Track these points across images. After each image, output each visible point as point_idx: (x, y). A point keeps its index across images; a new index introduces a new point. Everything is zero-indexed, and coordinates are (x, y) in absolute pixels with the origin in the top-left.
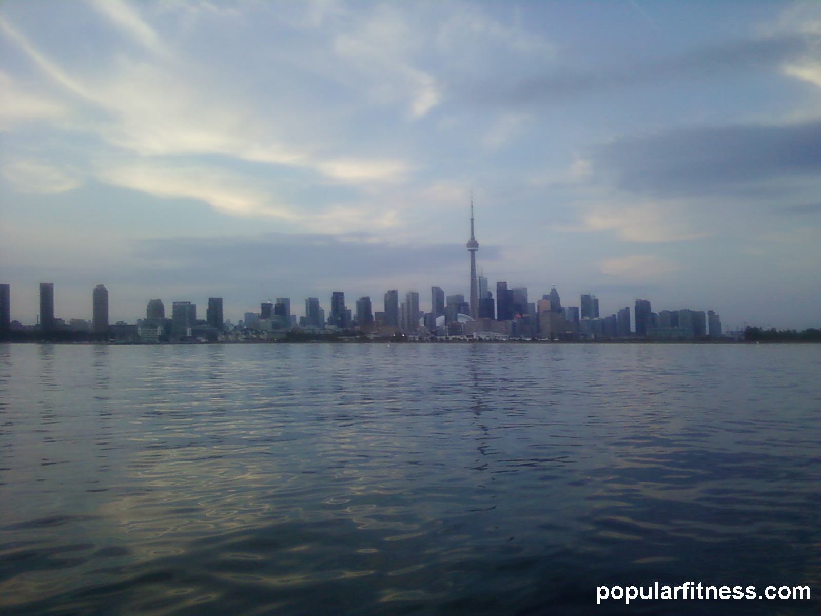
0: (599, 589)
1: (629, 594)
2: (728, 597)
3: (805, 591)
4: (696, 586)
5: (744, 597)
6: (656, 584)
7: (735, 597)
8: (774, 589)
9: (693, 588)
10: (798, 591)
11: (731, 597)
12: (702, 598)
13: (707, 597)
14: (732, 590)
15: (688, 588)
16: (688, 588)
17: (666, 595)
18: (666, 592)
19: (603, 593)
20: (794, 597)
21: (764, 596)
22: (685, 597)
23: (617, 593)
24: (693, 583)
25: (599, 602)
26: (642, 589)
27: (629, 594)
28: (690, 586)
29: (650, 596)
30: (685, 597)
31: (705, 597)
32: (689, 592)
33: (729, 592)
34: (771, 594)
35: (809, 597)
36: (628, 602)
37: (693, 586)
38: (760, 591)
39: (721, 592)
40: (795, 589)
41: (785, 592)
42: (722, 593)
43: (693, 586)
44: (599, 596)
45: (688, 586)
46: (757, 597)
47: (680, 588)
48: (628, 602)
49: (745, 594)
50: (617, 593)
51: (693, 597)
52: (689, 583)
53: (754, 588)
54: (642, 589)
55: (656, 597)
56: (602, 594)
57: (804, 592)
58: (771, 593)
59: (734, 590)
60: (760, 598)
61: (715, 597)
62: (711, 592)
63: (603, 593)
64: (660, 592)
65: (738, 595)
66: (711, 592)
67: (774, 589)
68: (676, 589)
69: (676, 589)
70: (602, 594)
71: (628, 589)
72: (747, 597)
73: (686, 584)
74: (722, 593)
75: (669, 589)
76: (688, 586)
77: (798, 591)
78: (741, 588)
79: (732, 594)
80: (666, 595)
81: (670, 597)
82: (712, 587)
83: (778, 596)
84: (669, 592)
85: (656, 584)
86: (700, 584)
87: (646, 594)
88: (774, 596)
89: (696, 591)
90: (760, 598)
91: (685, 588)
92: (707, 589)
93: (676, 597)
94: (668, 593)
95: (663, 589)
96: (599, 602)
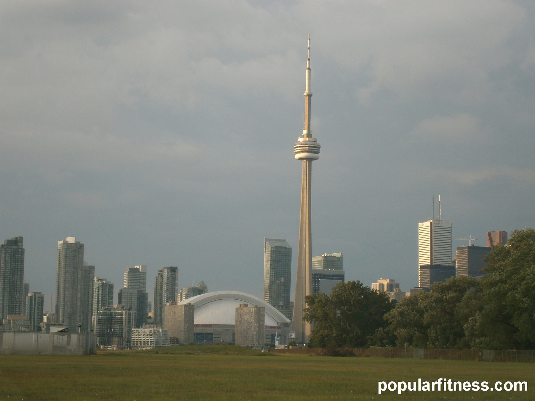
0: (380, 384)
2: (469, 389)
3: (523, 385)
4: (447, 381)
5: (480, 389)
6: (420, 380)
7: (473, 389)
8: (501, 383)
10: (518, 385)
11: (471, 390)
12: (452, 390)
13: (455, 389)
15: (441, 383)
16: (441, 383)
17: (426, 388)
19: (383, 386)
20: (515, 389)
21: (494, 389)
23: (392, 386)
24: (445, 380)
25: (380, 393)
28: (443, 381)
32: (442, 385)
33: (469, 385)
34: (499, 388)
35: (526, 389)
36: (399, 393)
38: (491, 385)
40: (516, 383)
41: (508, 386)
42: (465, 386)
44: (380, 390)
46: (489, 389)
47: (436, 383)
48: (399, 393)
49: (481, 387)
50: (392, 386)
51: (445, 389)
52: (442, 379)
53: (487, 383)
55: (420, 389)
56: (383, 386)
58: (499, 386)
60: (492, 389)
62: (458, 385)
63: (383, 386)
64: (422, 385)
66: (458, 385)
67: (501, 383)
68: (434, 384)
69: (434, 384)
70: (383, 386)
71: (400, 383)
72: (482, 389)
74: (465, 386)
75: (428, 383)
77: (518, 385)
79: (472, 387)
84: (428, 386)
85: (420, 380)
86: (450, 380)
88: (501, 389)
89: (447, 385)
90: (492, 389)
91: (439, 382)
92: (455, 383)
93: (433, 389)
94: (427, 387)
95: (424, 383)
96: (380, 393)
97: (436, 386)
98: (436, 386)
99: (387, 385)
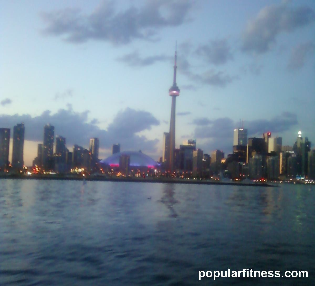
0: (200, 272)
1: (215, 275)
2: (266, 276)
3: (305, 273)
4: (249, 270)
5: (274, 276)
6: (229, 270)
7: (269, 276)
8: (290, 272)
9: (248, 272)
10: (302, 273)
11: (267, 276)
12: (253, 277)
13: (255, 277)
14: (268, 273)
15: (245, 272)
16: (245, 272)
17: (234, 275)
18: (234, 274)
20: (300, 276)
21: (284, 276)
22: (244, 276)
24: (248, 269)
25: (200, 279)
26: (222, 272)
27: (215, 275)
28: (246, 271)
29: (226, 276)
30: (244, 276)
31: (254, 276)
32: (246, 274)
33: (266, 274)
34: (288, 275)
35: (307, 276)
36: (214, 279)
37: (248, 270)
38: (282, 273)
39: (262, 274)
40: (300, 272)
41: (294, 274)
42: (263, 274)
43: (248, 270)
44: (200, 276)
45: (245, 271)
46: (281, 276)
47: (241, 272)
48: (214, 279)
49: (275, 274)
51: (248, 276)
52: (246, 269)
53: (279, 272)
54: (222, 272)
55: (229, 277)
56: (201, 275)
57: (305, 274)
58: (288, 274)
59: (269, 273)
60: (282, 277)
61: (259, 276)
62: (257, 274)
64: (231, 274)
65: (271, 275)
66: (257, 274)
67: (290, 272)
68: (239, 272)
69: (239, 272)
70: (201, 275)
71: (215, 272)
72: (276, 276)
73: (244, 269)
74: (263, 274)
75: (236, 272)
76: (245, 271)
77: (302, 273)
78: (272, 272)
79: (268, 275)
80: (234, 275)
81: (236, 276)
82: (258, 271)
83: (291, 276)
84: (236, 274)
85: (229, 270)
86: (251, 270)
87: (224, 275)
88: (290, 276)
89: (250, 273)
90: (282, 277)
91: (244, 272)
92: (255, 272)
93: (239, 276)
94: (235, 274)
95: (233, 272)
96: (200, 279)
97: (242, 274)
98: (242, 274)
99: (206, 275)
